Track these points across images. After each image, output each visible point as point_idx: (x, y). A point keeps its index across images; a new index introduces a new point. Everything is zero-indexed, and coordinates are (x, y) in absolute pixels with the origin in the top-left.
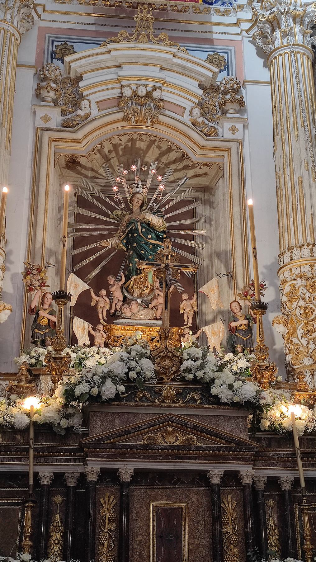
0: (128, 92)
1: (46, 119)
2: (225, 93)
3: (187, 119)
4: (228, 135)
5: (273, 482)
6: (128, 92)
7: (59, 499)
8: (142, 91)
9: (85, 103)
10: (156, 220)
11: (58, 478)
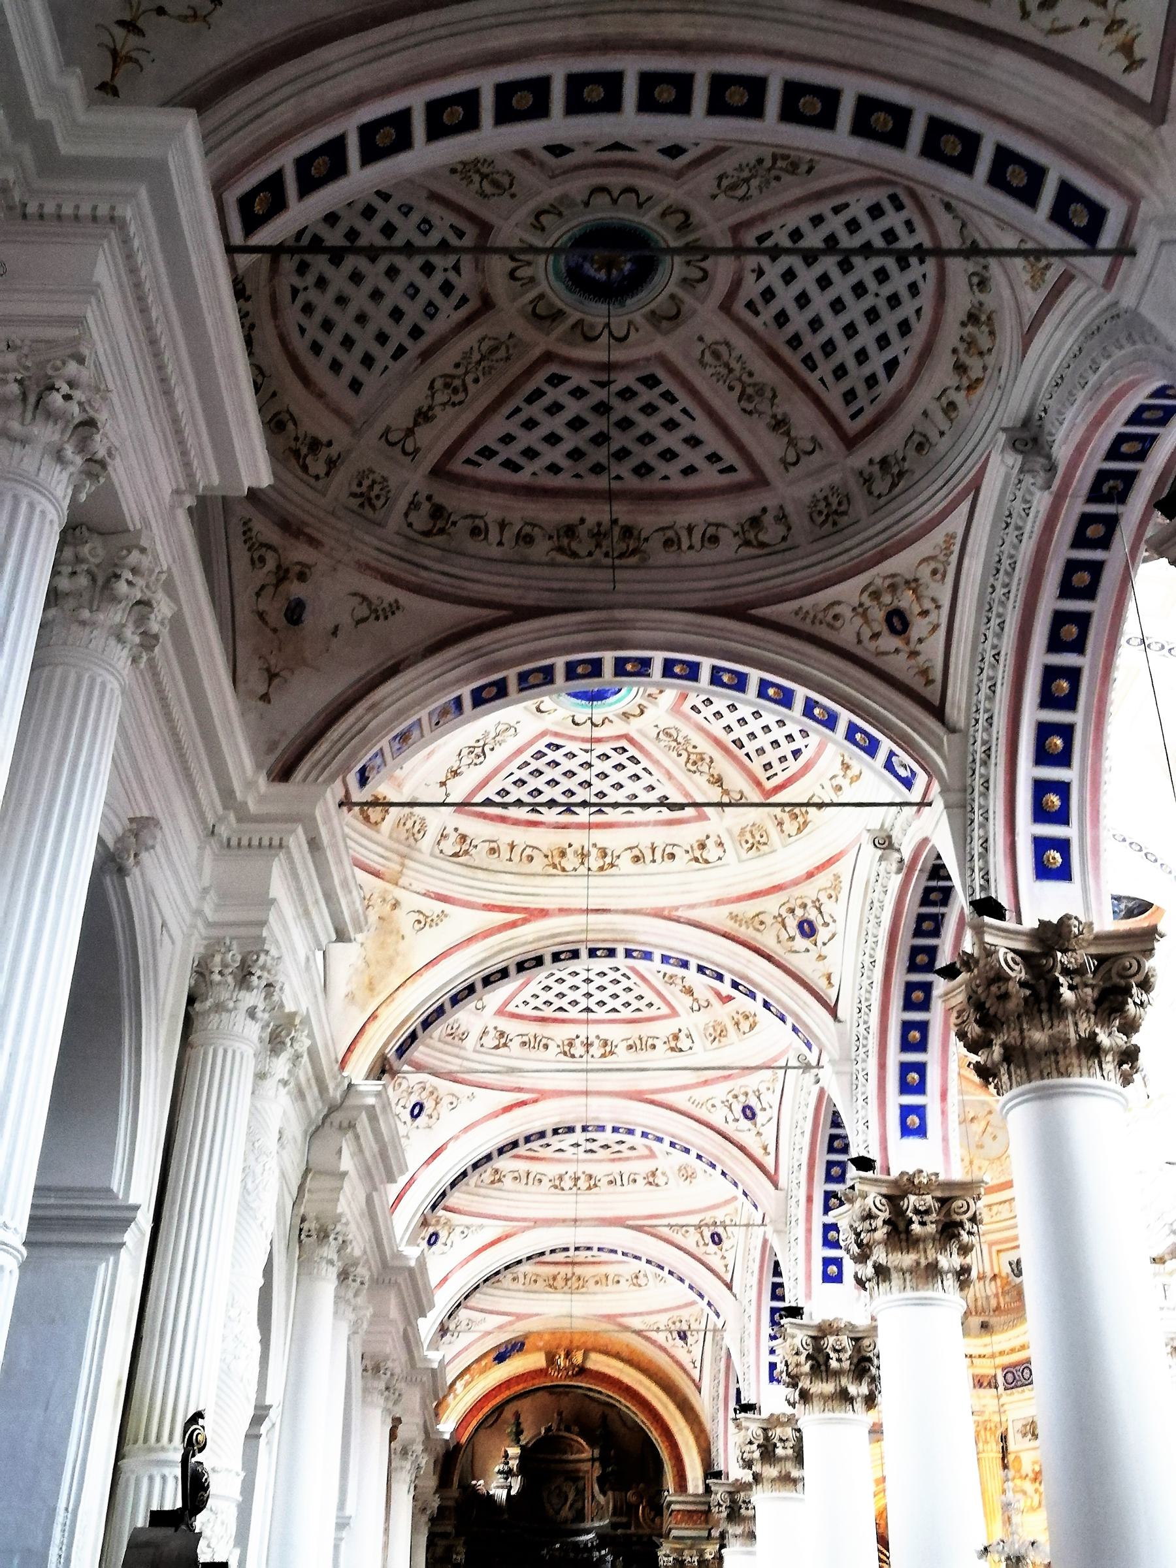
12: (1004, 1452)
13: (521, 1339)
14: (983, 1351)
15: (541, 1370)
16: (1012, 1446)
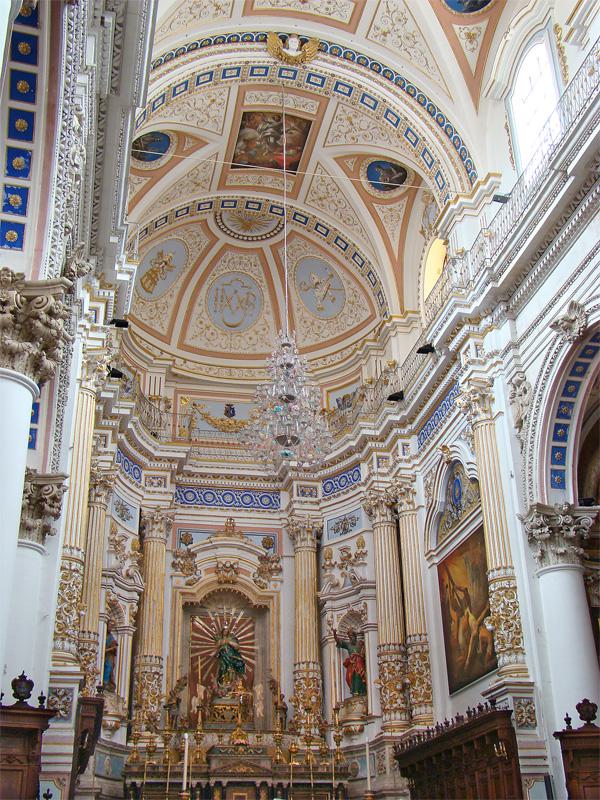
0: (220, 566)
2: (272, 562)
6: (220, 566)
7: (198, 792)
8: (228, 565)
11: (199, 784)
12: (319, 548)
16: (325, 541)
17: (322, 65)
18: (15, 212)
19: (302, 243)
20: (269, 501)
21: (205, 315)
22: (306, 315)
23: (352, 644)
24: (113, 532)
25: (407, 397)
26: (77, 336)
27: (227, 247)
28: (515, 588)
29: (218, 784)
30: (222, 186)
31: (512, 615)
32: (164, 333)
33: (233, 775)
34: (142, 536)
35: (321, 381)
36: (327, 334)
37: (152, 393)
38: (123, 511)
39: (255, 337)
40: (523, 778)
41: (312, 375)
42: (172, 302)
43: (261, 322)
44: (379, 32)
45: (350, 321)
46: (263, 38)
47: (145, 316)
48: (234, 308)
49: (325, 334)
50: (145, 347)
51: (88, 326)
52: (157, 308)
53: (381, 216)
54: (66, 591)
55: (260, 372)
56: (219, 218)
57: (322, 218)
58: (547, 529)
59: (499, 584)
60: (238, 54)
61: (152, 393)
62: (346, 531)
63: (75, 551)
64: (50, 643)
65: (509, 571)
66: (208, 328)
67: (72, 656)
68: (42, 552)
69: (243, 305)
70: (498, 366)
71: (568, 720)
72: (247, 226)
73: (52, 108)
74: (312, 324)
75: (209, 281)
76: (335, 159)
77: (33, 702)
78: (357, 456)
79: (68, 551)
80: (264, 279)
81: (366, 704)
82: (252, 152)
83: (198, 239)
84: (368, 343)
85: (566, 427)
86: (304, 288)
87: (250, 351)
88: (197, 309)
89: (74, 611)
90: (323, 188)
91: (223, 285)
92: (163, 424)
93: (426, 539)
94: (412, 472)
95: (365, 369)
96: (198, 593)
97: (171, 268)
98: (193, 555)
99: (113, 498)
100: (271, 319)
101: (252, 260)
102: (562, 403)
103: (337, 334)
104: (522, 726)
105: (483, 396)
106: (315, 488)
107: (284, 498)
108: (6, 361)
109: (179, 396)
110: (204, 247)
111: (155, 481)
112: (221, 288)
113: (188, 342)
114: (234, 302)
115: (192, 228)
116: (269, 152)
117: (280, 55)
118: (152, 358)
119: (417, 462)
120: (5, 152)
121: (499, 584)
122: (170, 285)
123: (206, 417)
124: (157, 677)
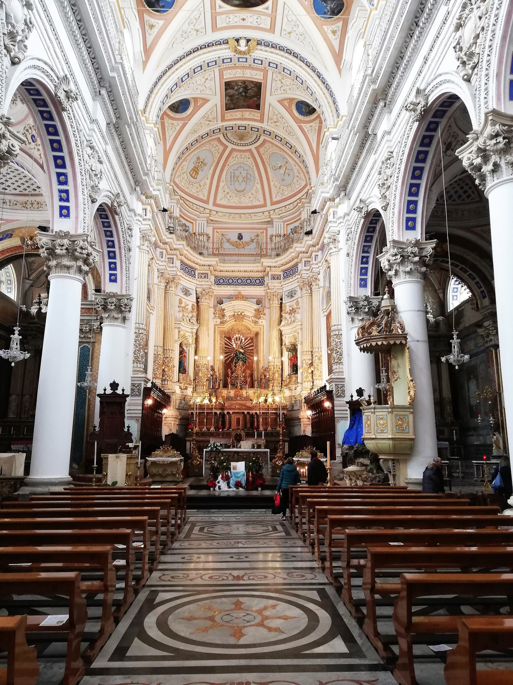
0: (236, 314)
1: (216, 322)
3: (251, 320)
4: (260, 324)
5: (256, 413)
6: (236, 314)
8: (239, 313)
9: (225, 317)
10: (242, 351)
12: (281, 303)
13: (10, 232)
14: (275, 264)
15: (20, 246)
16: (284, 302)
17: (260, 53)
18: (65, 201)
19: (270, 145)
20: (261, 282)
21: (226, 187)
22: (276, 183)
23: (294, 349)
24: (180, 302)
25: (314, 232)
26: (135, 225)
27: (232, 150)
28: (341, 334)
29: (228, 413)
30: (223, 120)
31: (339, 347)
32: (205, 198)
33: (234, 409)
34: (198, 302)
35: (284, 219)
36: (287, 194)
37: (200, 232)
38: (186, 292)
39: (252, 197)
40: (336, 419)
41: (279, 216)
42: (208, 182)
43: (255, 188)
44: (286, 32)
45: (297, 186)
46: (226, 42)
47: (194, 191)
48: (240, 181)
49: (286, 194)
50: (195, 208)
51: (141, 219)
52: (200, 186)
53: (306, 130)
54: (138, 342)
55: (255, 216)
56: (225, 136)
57: (277, 132)
58: (353, 309)
59: (334, 333)
60: (214, 53)
61: (200, 232)
62: (292, 297)
63: (141, 325)
64: (132, 365)
65: (339, 326)
66: (228, 193)
67: (142, 370)
68: (124, 327)
69: (245, 179)
70: (342, 224)
71: (352, 396)
72: (241, 138)
73: (71, 153)
74: (280, 188)
75: (226, 168)
76: (278, 101)
77: (119, 391)
78: (296, 260)
79: (137, 325)
80: (254, 166)
81: (297, 378)
82: (234, 101)
83: (217, 148)
84: (303, 200)
85: (367, 257)
86: (275, 169)
87: (250, 204)
88: (222, 184)
89: (142, 351)
90: (275, 117)
91: (234, 170)
92: (205, 247)
93: (323, 303)
94: (318, 270)
95: (303, 213)
96: (227, 327)
97: (205, 164)
98: (224, 310)
99: (180, 287)
100: (259, 186)
101: (247, 156)
102: (364, 246)
103: (291, 194)
104: (338, 397)
105: (335, 240)
106: (280, 275)
107: (266, 279)
108: (66, 271)
109: (215, 231)
110: (221, 151)
111: (203, 276)
112: (232, 171)
113: (218, 202)
114: (240, 179)
115: (212, 143)
116: (244, 100)
117: (236, 51)
118: (199, 213)
119: (320, 264)
120: (55, 174)
121: (334, 333)
122: (205, 174)
123: (228, 241)
124: (205, 366)
